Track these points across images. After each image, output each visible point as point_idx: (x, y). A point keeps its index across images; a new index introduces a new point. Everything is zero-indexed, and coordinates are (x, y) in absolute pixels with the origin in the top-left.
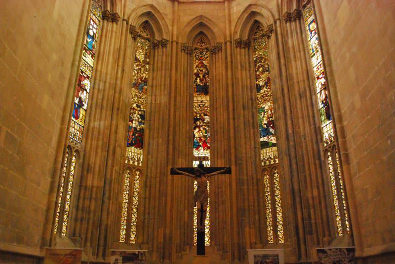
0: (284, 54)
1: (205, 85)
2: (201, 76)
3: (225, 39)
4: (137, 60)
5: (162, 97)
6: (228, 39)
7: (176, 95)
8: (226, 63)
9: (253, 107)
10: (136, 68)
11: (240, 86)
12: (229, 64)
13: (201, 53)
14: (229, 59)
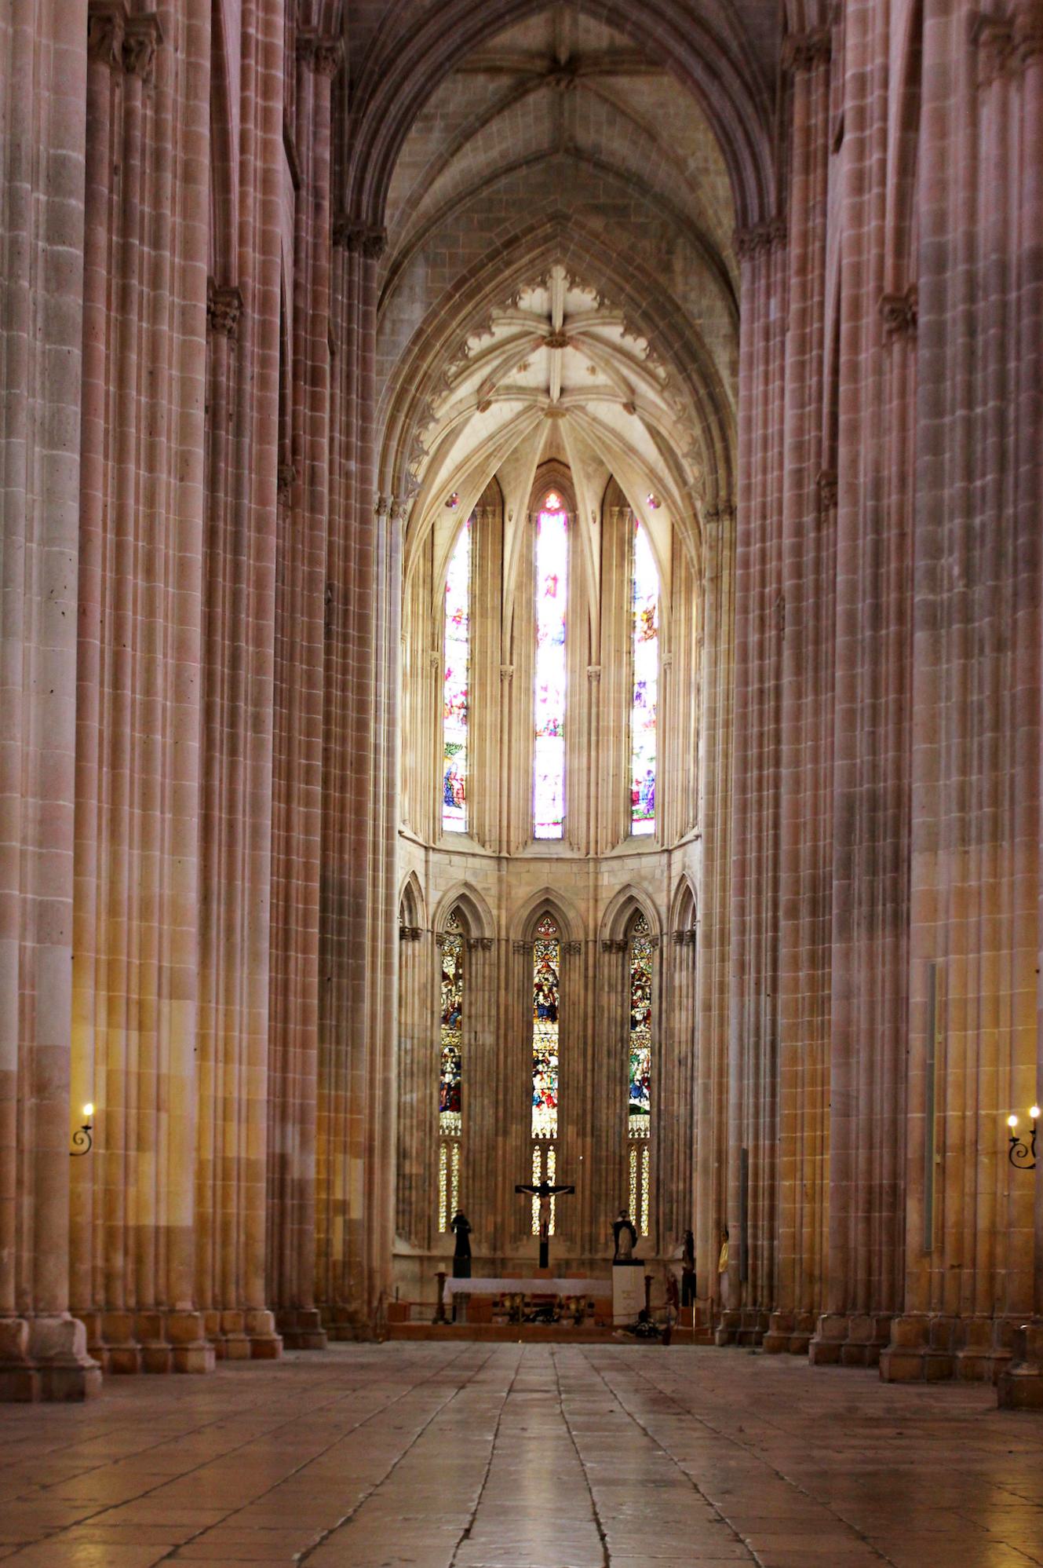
0: (666, 991)
1: (552, 1005)
2: (546, 989)
3: (587, 934)
4: (445, 976)
5: (487, 1035)
6: (591, 937)
7: (506, 1030)
8: (586, 977)
9: (622, 1053)
10: (445, 990)
11: (606, 1020)
12: (590, 980)
13: (546, 947)
14: (591, 973)
